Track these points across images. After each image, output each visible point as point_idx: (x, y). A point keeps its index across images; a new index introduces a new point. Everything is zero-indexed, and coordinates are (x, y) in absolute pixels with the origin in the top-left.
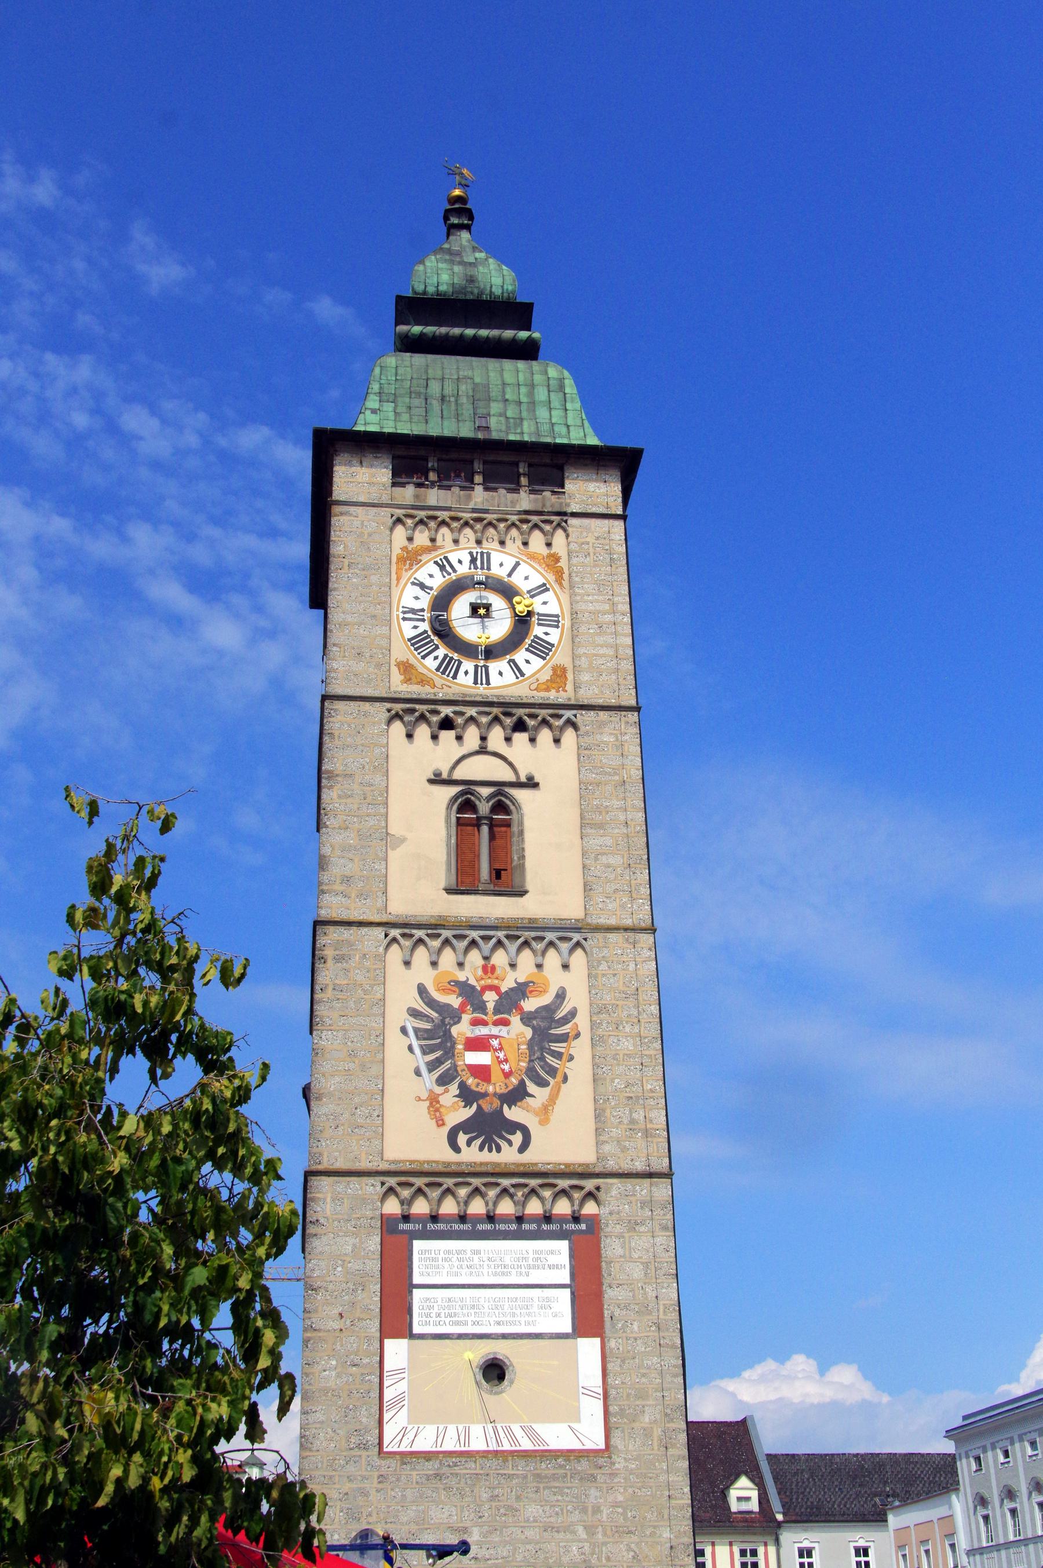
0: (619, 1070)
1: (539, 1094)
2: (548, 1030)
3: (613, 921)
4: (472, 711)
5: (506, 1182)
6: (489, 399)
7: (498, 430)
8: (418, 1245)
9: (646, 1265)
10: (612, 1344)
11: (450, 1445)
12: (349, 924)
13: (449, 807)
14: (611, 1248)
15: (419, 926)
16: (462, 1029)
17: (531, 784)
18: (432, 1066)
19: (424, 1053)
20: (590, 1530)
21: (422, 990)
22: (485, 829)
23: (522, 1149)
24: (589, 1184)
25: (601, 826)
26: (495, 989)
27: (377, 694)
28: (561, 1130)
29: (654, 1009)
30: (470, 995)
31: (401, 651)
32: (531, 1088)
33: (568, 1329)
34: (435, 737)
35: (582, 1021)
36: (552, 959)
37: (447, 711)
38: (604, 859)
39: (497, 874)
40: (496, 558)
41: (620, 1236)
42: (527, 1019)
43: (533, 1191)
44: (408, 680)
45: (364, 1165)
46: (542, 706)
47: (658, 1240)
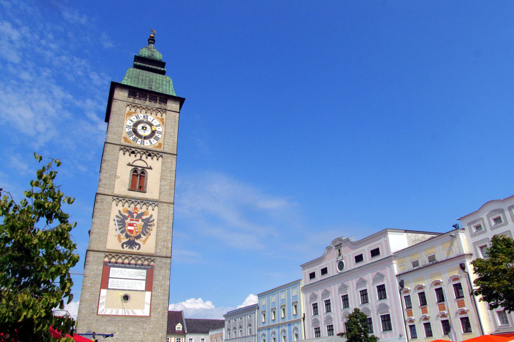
0: (162, 234)
1: (143, 237)
2: (148, 223)
3: (165, 201)
4: (139, 150)
5: (134, 256)
6: (153, 82)
7: (154, 89)
8: (112, 269)
9: (163, 277)
10: (154, 293)
11: (114, 313)
12: (104, 195)
13: (131, 171)
14: (156, 272)
15: (121, 197)
16: (128, 221)
17: (150, 168)
18: (120, 229)
19: (119, 225)
20: (144, 333)
21: (120, 211)
22: (139, 177)
23: (138, 249)
24: (153, 258)
25: (165, 179)
26: (137, 213)
27: (118, 143)
28: (148, 245)
29: (172, 221)
30: (131, 214)
31: (124, 135)
32: (142, 236)
33: (144, 289)
34: (130, 155)
35: (155, 222)
36: (150, 208)
37: (133, 149)
38: (165, 187)
39: (140, 187)
40: (149, 117)
41: (158, 270)
42: (143, 220)
43: (140, 259)
44: (125, 141)
45: (101, 249)
46: (155, 151)
47: (167, 271)
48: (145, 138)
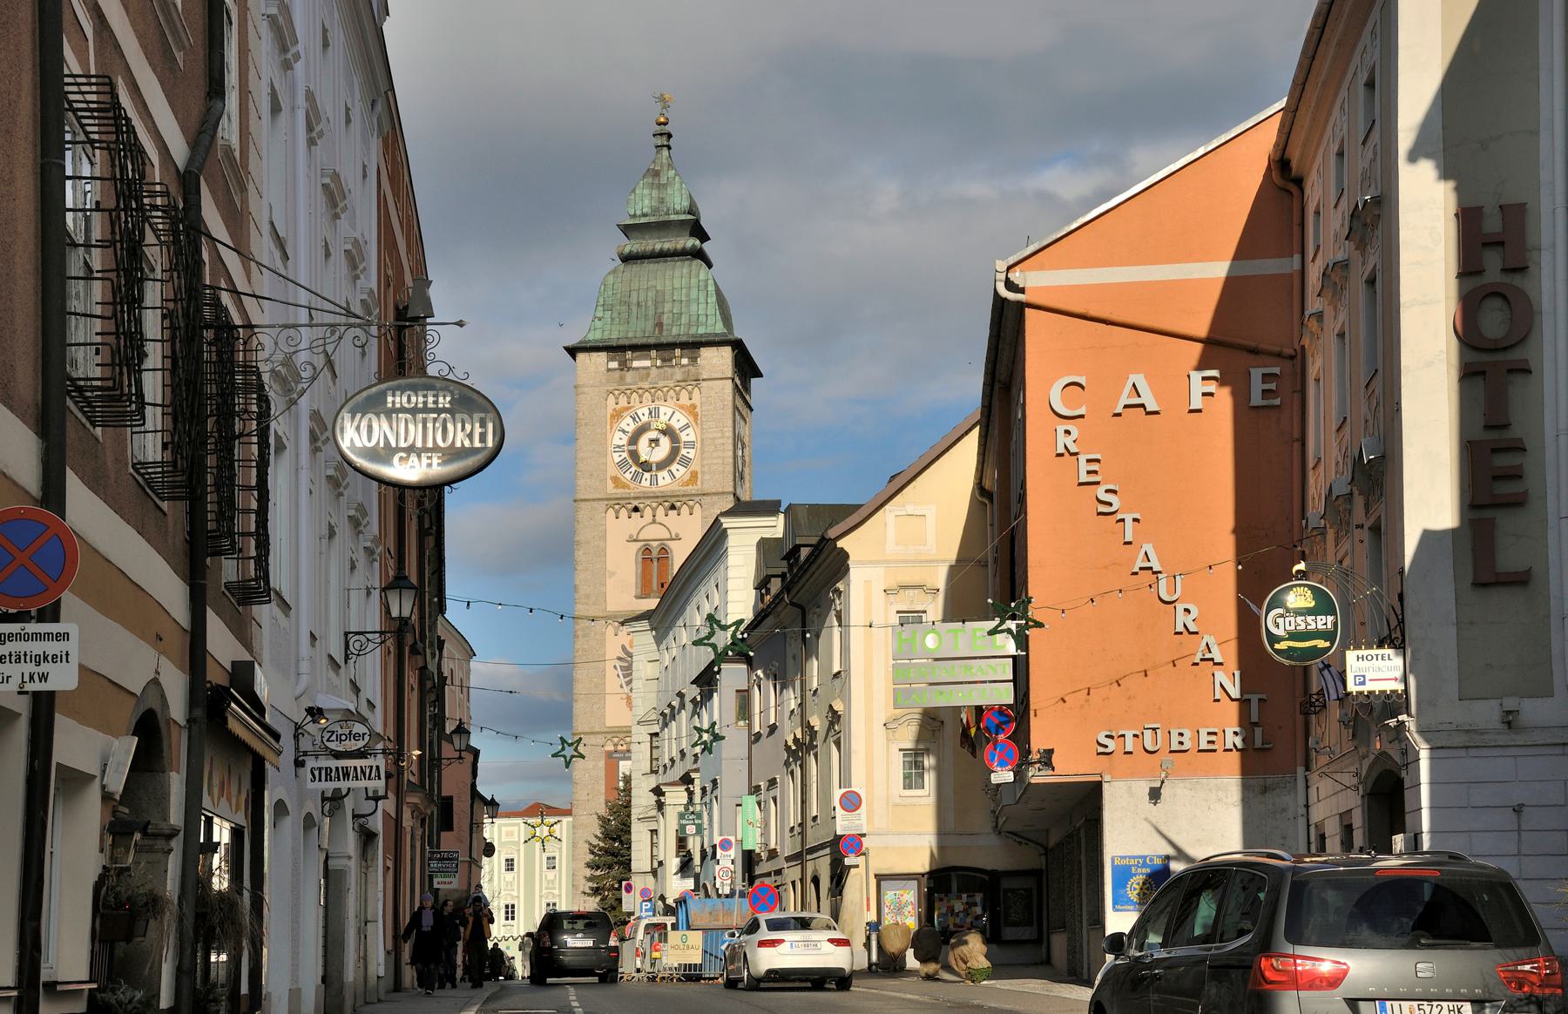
21: (623, 648)
31: (612, 471)
37: (635, 503)
40: (662, 410)
48: (662, 465)
